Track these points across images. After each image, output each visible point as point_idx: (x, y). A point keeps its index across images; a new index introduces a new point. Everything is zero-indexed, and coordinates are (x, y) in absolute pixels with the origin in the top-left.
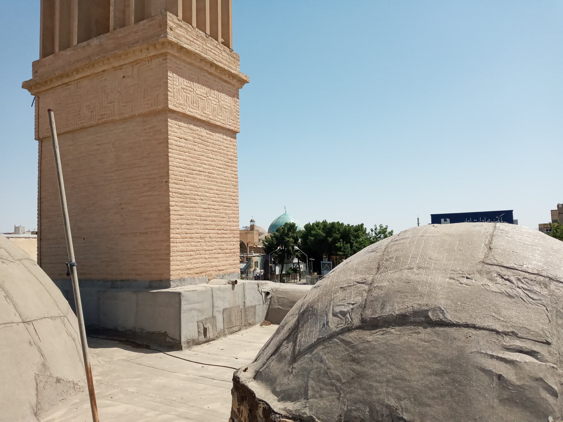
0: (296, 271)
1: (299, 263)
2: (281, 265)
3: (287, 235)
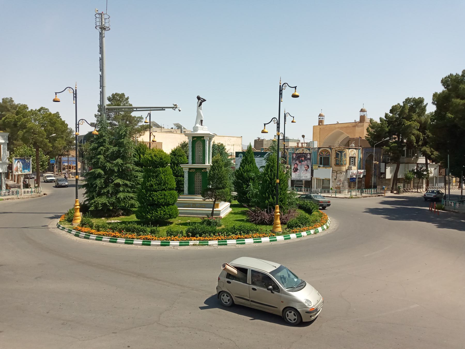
0: (420, 174)
1: (427, 164)
2: (395, 166)
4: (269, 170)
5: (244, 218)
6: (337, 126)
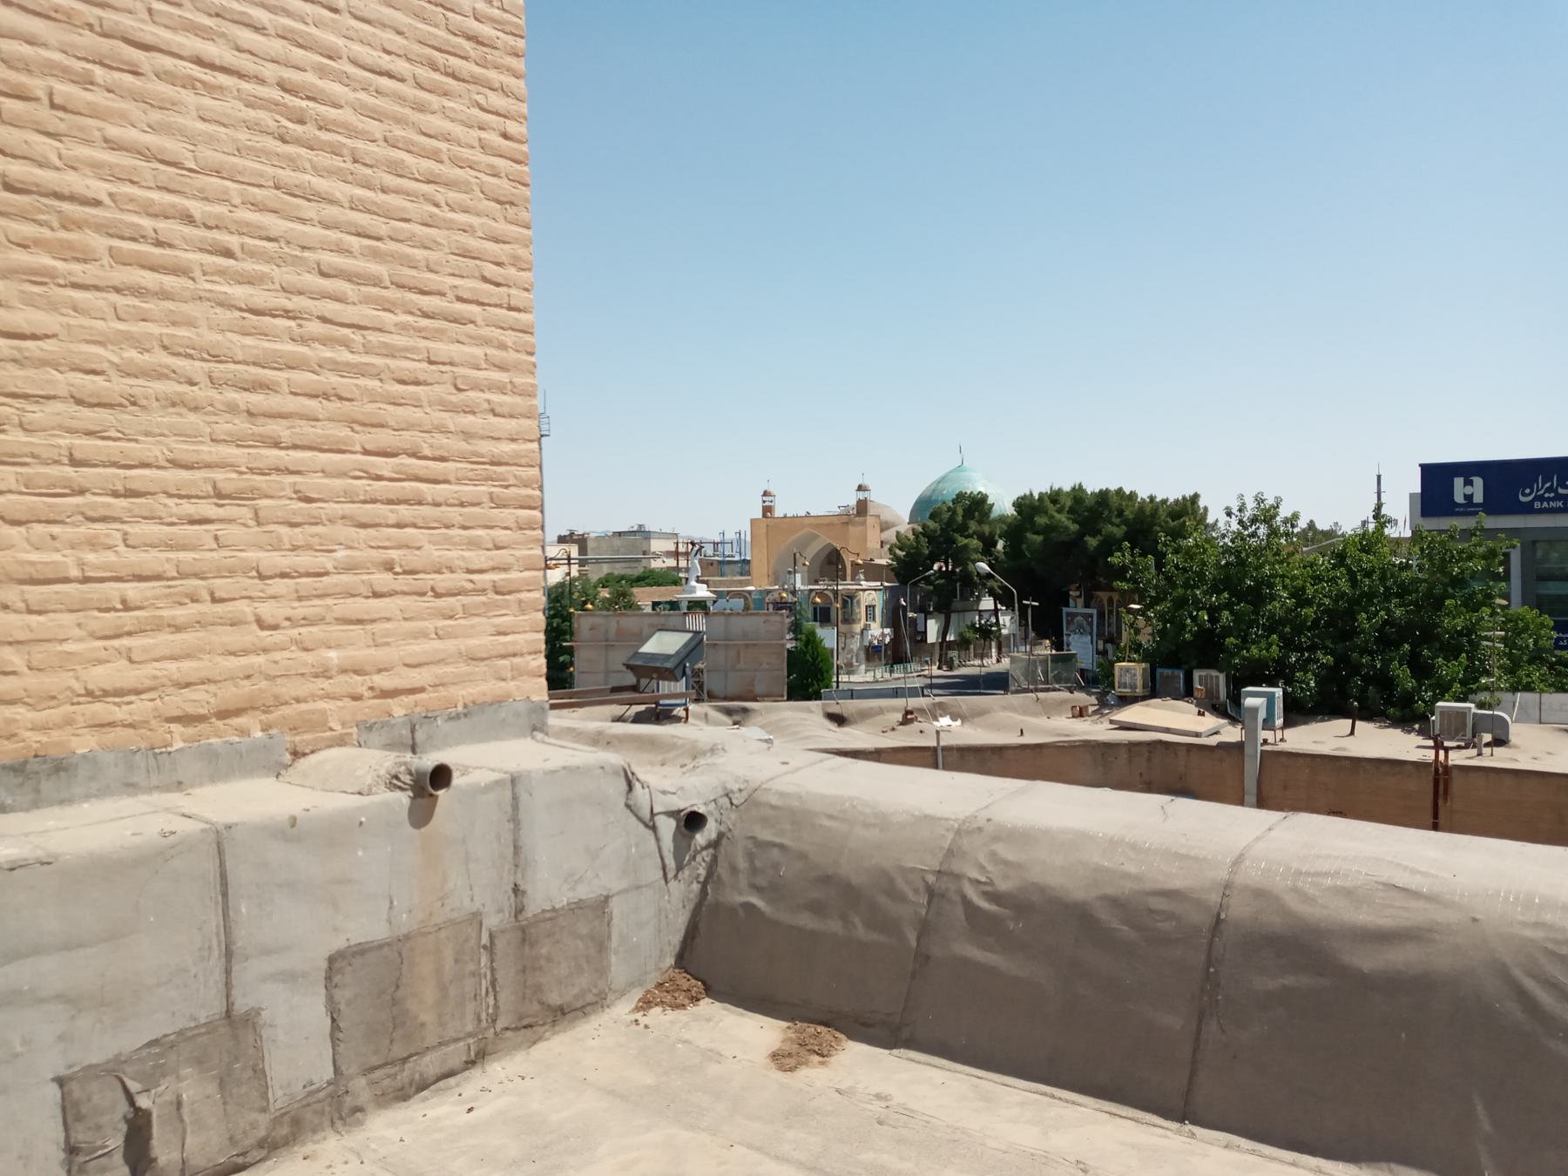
0: (987, 632)
1: (996, 611)
3: (963, 529)
6: (806, 521)
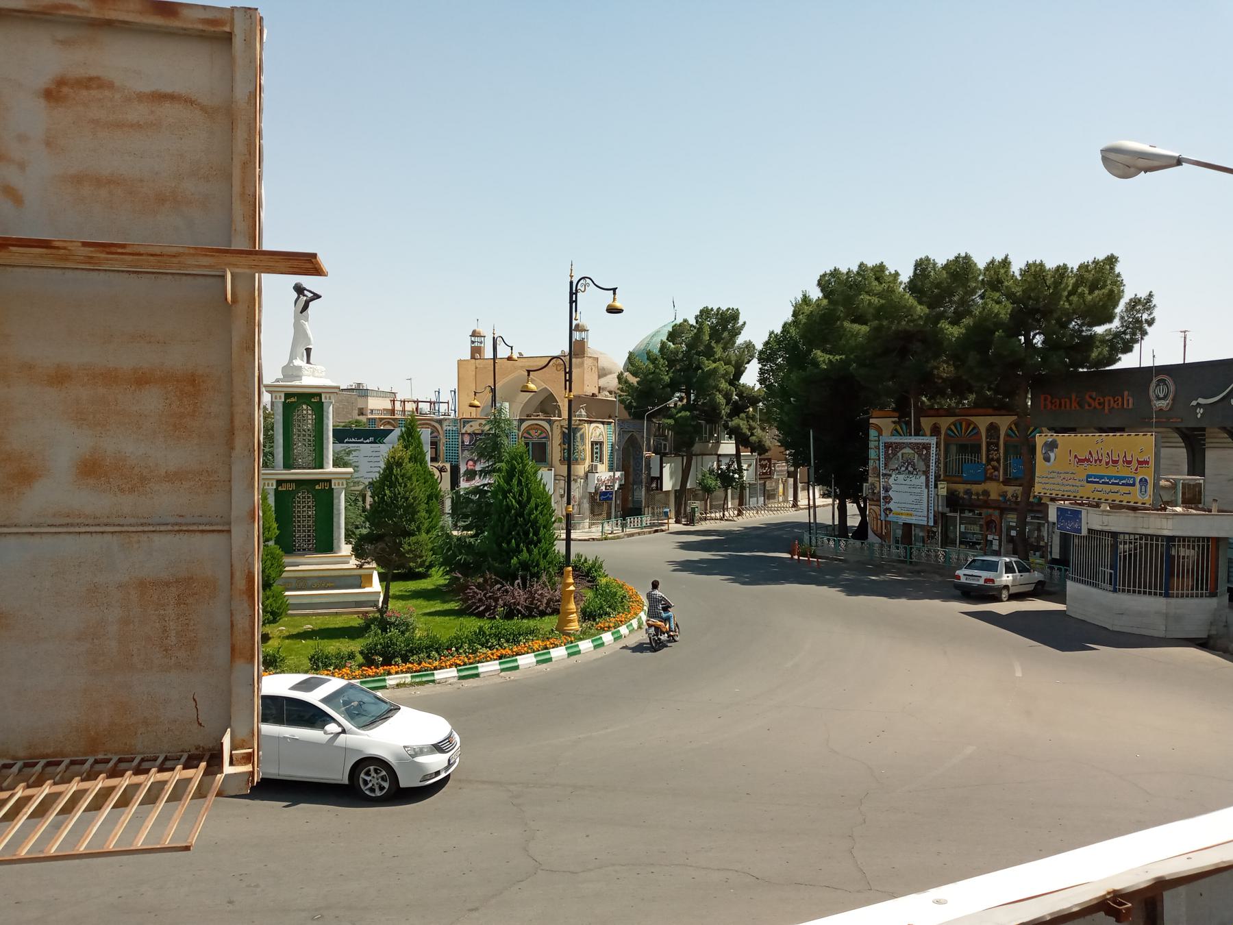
0: (726, 479)
3: (709, 353)
4: (515, 481)
5: (438, 606)
